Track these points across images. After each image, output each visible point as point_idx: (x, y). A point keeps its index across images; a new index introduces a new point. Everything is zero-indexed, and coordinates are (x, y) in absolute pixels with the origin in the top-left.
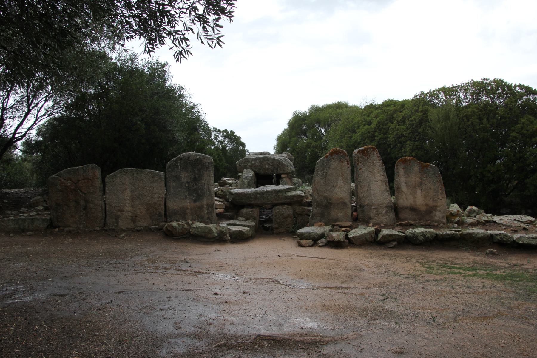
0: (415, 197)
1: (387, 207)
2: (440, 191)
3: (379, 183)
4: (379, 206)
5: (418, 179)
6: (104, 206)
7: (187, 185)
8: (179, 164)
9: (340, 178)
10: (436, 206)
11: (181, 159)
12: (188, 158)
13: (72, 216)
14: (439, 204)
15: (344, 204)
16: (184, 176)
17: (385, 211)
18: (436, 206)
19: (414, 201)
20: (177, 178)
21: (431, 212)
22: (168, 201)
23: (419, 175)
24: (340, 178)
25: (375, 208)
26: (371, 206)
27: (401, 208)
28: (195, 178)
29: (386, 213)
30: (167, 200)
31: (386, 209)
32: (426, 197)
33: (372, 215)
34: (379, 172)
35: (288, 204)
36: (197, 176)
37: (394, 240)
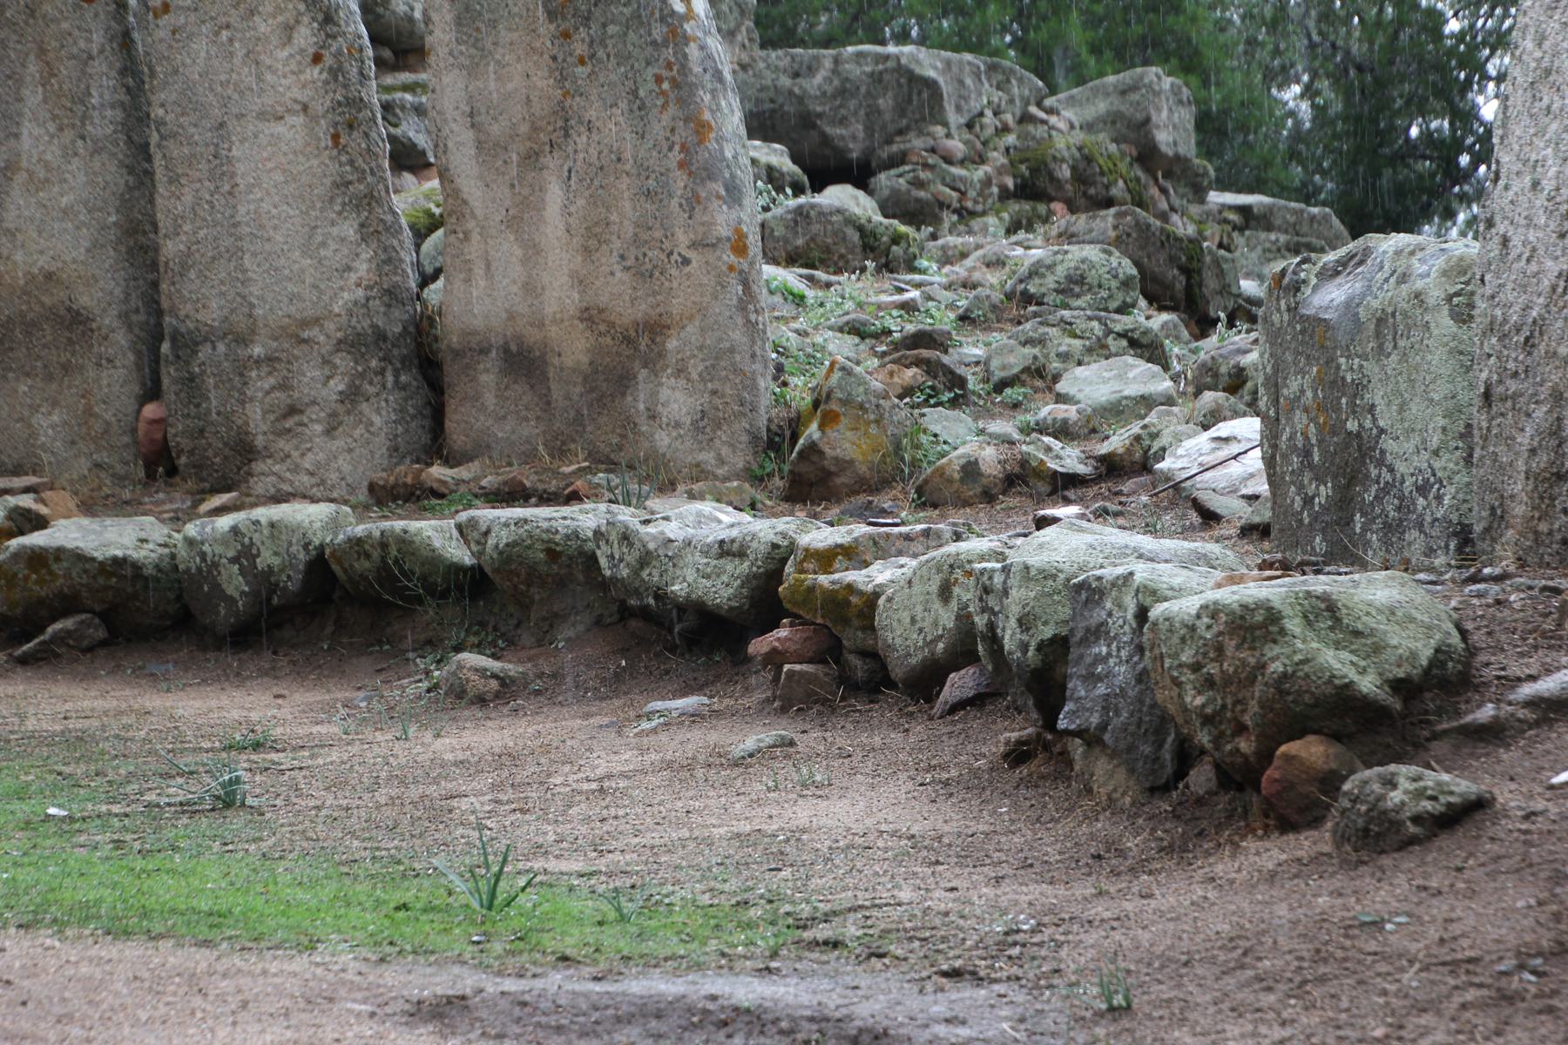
0: (533, 252)
1: (353, 344)
2: (680, 181)
3: (292, 130)
4: (296, 334)
5: (543, 82)
9: (33, 97)
10: (656, 328)
14: (677, 305)
15: (75, 322)
17: (338, 385)
18: (656, 328)
19: (531, 288)
21: (624, 381)
23: (546, 28)
24: (33, 97)
25: (270, 360)
26: (243, 340)
27: (458, 354)
29: (352, 396)
31: (343, 361)
32: (592, 238)
33: (256, 419)
34: (289, 29)
37: (67, 604)
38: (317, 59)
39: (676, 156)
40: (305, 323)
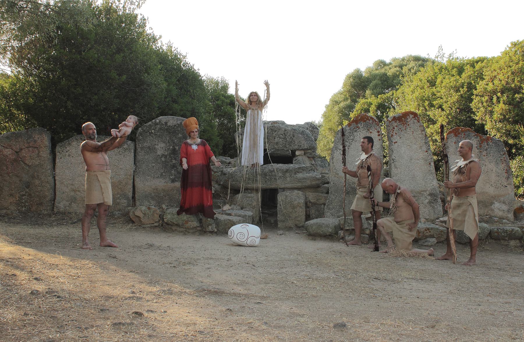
6: (53, 184)
7: (163, 159)
8: (153, 131)
11: (156, 124)
12: (166, 123)
13: (11, 195)
16: (161, 148)
20: (151, 149)
22: (137, 180)
28: (174, 150)
30: (135, 178)
35: (299, 189)
36: (177, 148)
38: (427, 151)
39: (505, 171)
40: (422, 191)
